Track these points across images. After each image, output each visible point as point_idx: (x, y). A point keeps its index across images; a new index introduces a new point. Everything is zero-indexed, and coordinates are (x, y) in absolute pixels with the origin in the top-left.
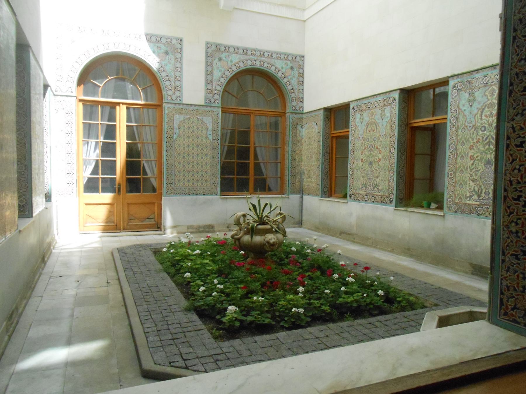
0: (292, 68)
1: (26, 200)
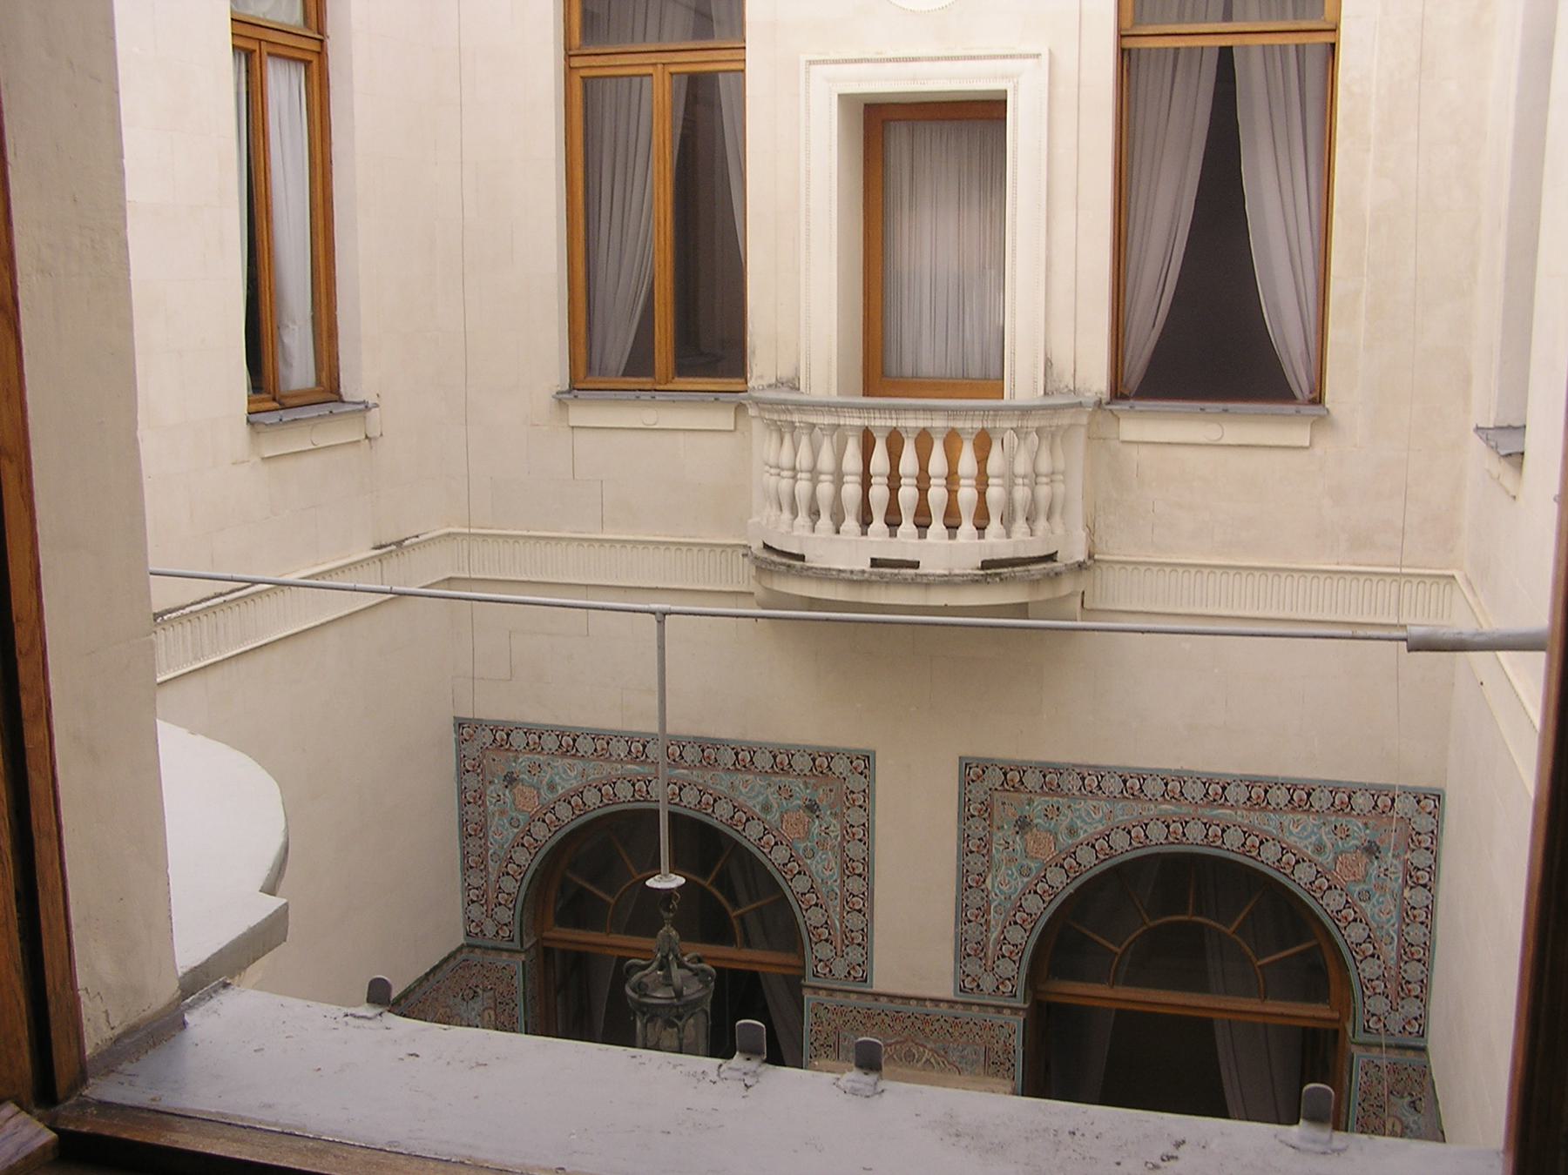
0: (1372, 850)
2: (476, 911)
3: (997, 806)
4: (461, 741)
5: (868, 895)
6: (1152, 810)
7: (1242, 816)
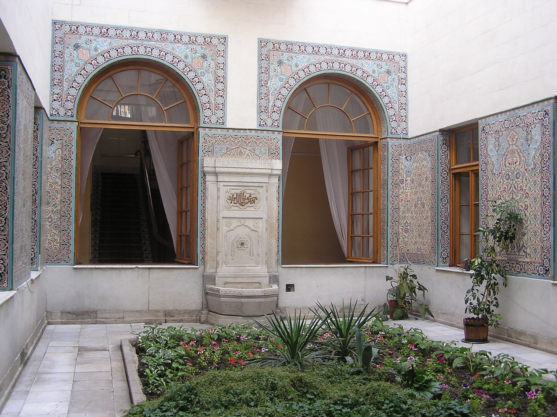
0: (389, 72)
1: (5, 267)
2: (56, 105)
3: (271, 56)
4: (55, 30)
5: (224, 90)
6: (322, 58)
7: (350, 61)
